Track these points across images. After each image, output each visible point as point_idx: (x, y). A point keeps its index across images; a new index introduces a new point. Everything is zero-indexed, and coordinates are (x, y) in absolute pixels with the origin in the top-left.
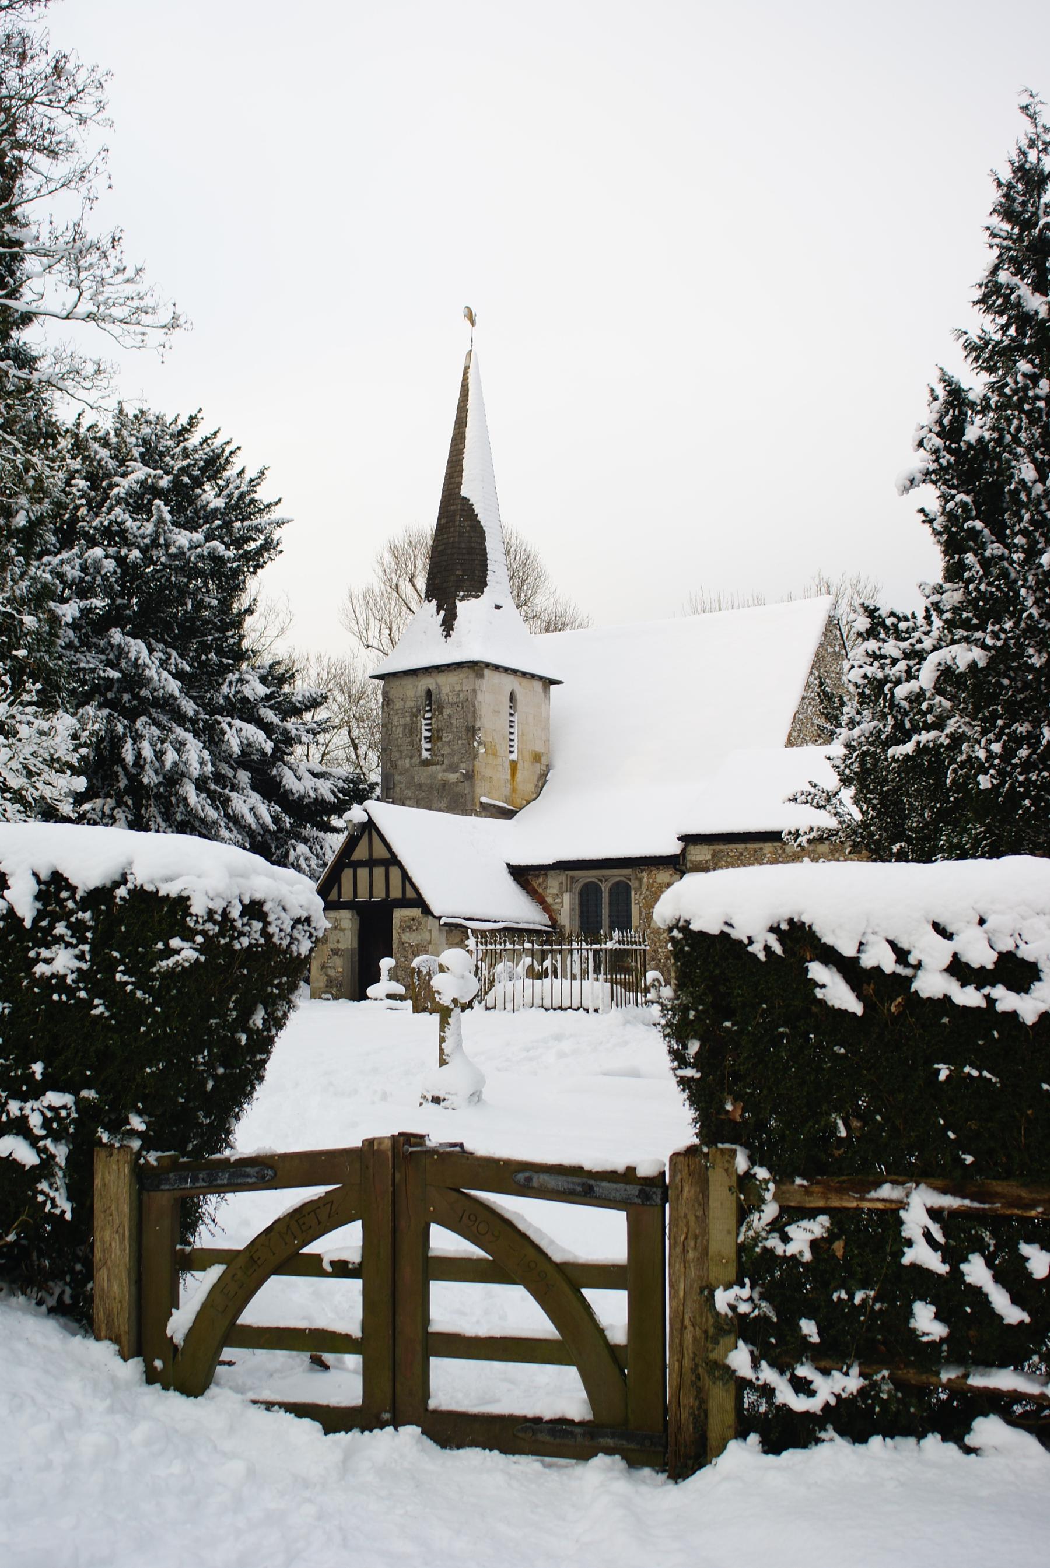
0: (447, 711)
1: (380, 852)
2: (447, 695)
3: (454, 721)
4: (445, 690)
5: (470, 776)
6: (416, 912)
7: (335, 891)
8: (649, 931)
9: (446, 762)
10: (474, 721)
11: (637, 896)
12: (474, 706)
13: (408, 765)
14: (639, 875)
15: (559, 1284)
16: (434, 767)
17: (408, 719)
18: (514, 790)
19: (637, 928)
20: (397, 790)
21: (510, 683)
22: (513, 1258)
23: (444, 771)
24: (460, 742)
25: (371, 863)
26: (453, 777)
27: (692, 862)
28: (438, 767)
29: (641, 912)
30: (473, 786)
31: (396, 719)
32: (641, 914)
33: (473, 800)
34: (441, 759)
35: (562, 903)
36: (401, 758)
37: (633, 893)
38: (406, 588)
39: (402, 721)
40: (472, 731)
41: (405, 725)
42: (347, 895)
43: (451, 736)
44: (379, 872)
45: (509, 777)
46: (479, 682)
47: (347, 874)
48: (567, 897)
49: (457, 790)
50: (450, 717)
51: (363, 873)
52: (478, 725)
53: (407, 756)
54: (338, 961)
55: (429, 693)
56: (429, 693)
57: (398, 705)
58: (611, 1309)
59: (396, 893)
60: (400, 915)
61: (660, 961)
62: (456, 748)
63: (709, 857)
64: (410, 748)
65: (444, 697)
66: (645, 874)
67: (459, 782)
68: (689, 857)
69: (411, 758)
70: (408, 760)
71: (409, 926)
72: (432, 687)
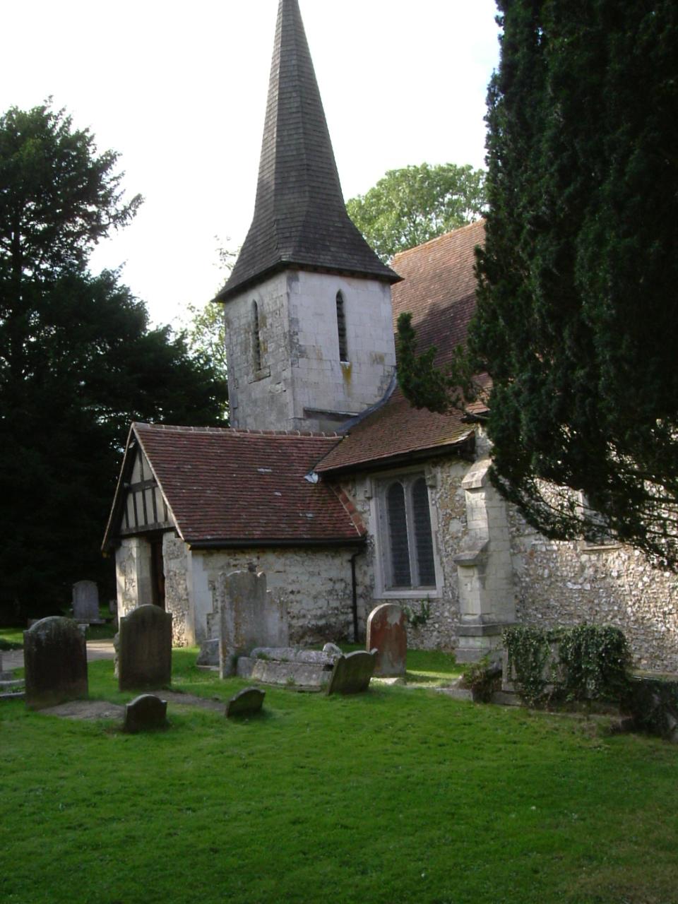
0: (269, 321)
3: (274, 330)
4: (266, 300)
7: (124, 520)
8: (447, 538)
11: (433, 495)
14: (434, 471)
16: (264, 380)
18: (349, 395)
19: (436, 532)
20: (241, 408)
21: (330, 285)
23: (271, 383)
32: (438, 518)
36: (241, 377)
37: (429, 492)
41: (241, 343)
45: (341, 381)
50: (271, 325)
55: (255, 305)
56: (255, 305)
57: (236, 325)
66: (439, 469)
72: (257, 299)
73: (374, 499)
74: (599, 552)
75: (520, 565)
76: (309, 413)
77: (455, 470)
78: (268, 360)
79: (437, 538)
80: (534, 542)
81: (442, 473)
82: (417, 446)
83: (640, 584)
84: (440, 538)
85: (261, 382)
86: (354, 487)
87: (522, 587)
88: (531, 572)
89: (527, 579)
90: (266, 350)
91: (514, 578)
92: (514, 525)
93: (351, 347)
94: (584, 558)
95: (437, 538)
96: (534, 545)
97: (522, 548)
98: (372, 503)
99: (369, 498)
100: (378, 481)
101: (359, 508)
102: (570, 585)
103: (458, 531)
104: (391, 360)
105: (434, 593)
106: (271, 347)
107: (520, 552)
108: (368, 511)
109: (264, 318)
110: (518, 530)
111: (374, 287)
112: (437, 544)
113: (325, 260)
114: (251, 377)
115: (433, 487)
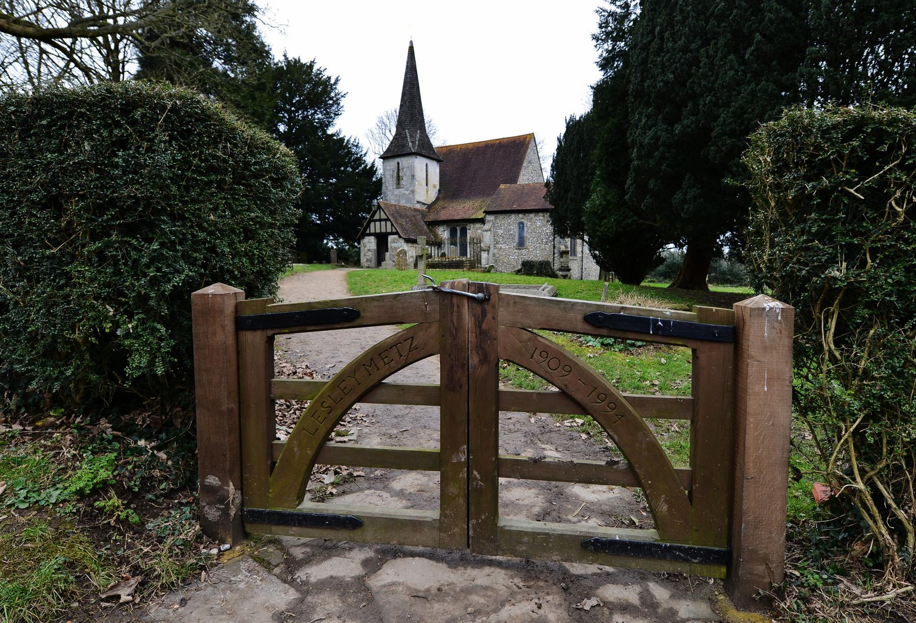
1: (383, 216)
5: (413, 192)
6: (396, 236)
15: (616, 415)
21: (425, 161)
22: (575, 396)
25: (380, 220)
38: (388, 134)
40: (413, 176)
42: (372, 231)
44: (383, 223)
47: (372, 224)
51: (378, 223)
54: (370, 253)
55: (398, 163)
56: (398, 163)
58: (673, 440)
59: (389, 230)
60: (390, 238)
71: (393, 242)
75: (496, 251)
76: (418, 202)
77: (478, 225)
78: (402, 182)
82: (474, 217)
91: (494, 255)
93: (429, 182)
100: (448, 226)
104: (438, 187)
106: (405, 178)
108: (444, 233)
111: (435, 163)
113: (424, 152)
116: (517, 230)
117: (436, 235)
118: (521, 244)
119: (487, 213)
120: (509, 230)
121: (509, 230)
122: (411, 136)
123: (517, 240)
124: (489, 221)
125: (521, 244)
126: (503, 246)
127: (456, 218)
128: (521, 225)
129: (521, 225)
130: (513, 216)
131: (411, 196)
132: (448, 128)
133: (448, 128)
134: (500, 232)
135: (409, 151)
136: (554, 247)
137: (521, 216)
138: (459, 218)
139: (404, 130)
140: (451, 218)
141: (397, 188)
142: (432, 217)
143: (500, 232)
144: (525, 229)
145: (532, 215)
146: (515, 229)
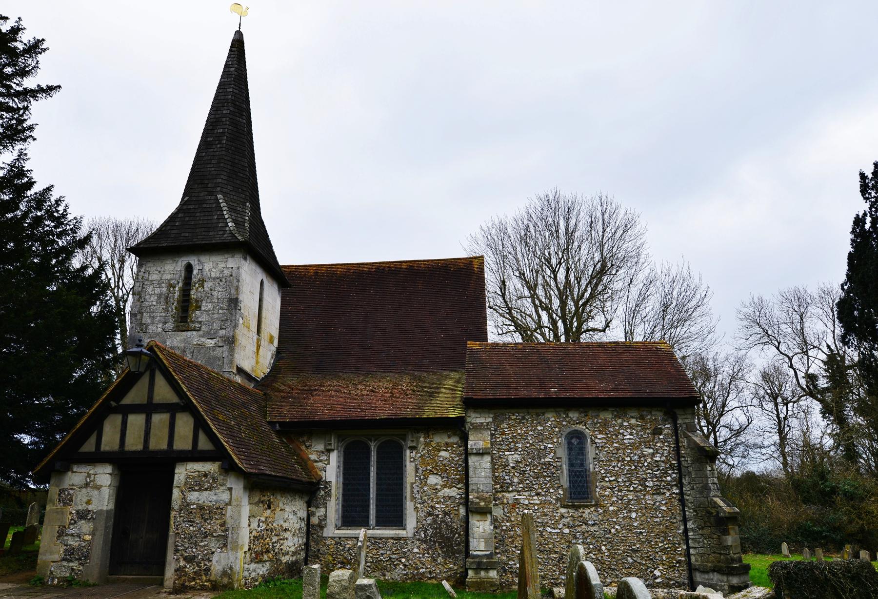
0: (208, 285)
2: (210, 270)
3: (215, 293)
5: (231, 342)
9: (203, 328)
10: (238, 294)
11: (413, 455)
12: (238, 281)
13: (160, 330)
14: (415, 435)
16: (189, 333)
17: (164, 289)
19: (412, 484)
24: (221, 311)
26: (211, 343)
27: (472, 424)
28: (195, 333)
29: (417, 470)
30: (232, 351)
31: (150, 288)
33: (231, 362)
34: (197, 325)
35: (328, 460)
36: (153, 323)
37: (408, 452)
39: (157, 291)
43: (210, 306)
46: (243, 262)
48: (334, 457)
49: (214, 354)
52: (241, 298)
53: (159, 321)
56: (189, 268)
61: (437, 516)
62: (216, 316)
63: (490, 420)
64: (163, 314)
65: (206, 273)
67: (217, 346)
68: (469, 420)
69: (165, 323)
70: (160, 325)
73: (335, 452)
74: (576, 508)
77: (440, 439)
79: (412, 488)
80: (517, 497)
81: (425, 438)
83: (613, 531)
84: (416, 490)
85: (184, 333)
86: (309, 439)
87: (503, 530)
88: (513, 519)
89: (508, 524)
90: (199, 307)
92: (496, 483)
94: (563, 510)
95: (412, 488)
96: (516, 499)
97: (505, 501)
98: (334, 457)
99: (329, 451)
100: (340, 438)
101: (313, 457)
102: (549, 529)
103: (436, 484)
105: (402, 533)
106: (206, 306)
107: (503, 503)
109: (202, 282)
110: (501, 487)
112: (412, 492)
114: (170, 326)
115: (412, 448)
116: (562, 453)
117: (305, 463)
118: (580, 491)
119: (470, 404)
120: (542, 453)
121: (542, 453)
122: (231, 209)
123: (565, 481)
124: (478, 428)
125: (580, 491)
126: (523, 498)
127: (369, 415)
128: (576, 444)
129: (576, 444)
130: (551, 418)
131: (224, 352)
132: (316, 212)
133: (316, 212)
134: (512, 458)
135: (227, 238)
136: (682, 502)
137: (574, 415)
138: (382, 414)
139: (212, 193)
140: (353, 414)
141: (178, 329)
142: (288, 413)
143: (512, 458)
144: (591, 451)
145: (607, 415)
146: (557, 451)
